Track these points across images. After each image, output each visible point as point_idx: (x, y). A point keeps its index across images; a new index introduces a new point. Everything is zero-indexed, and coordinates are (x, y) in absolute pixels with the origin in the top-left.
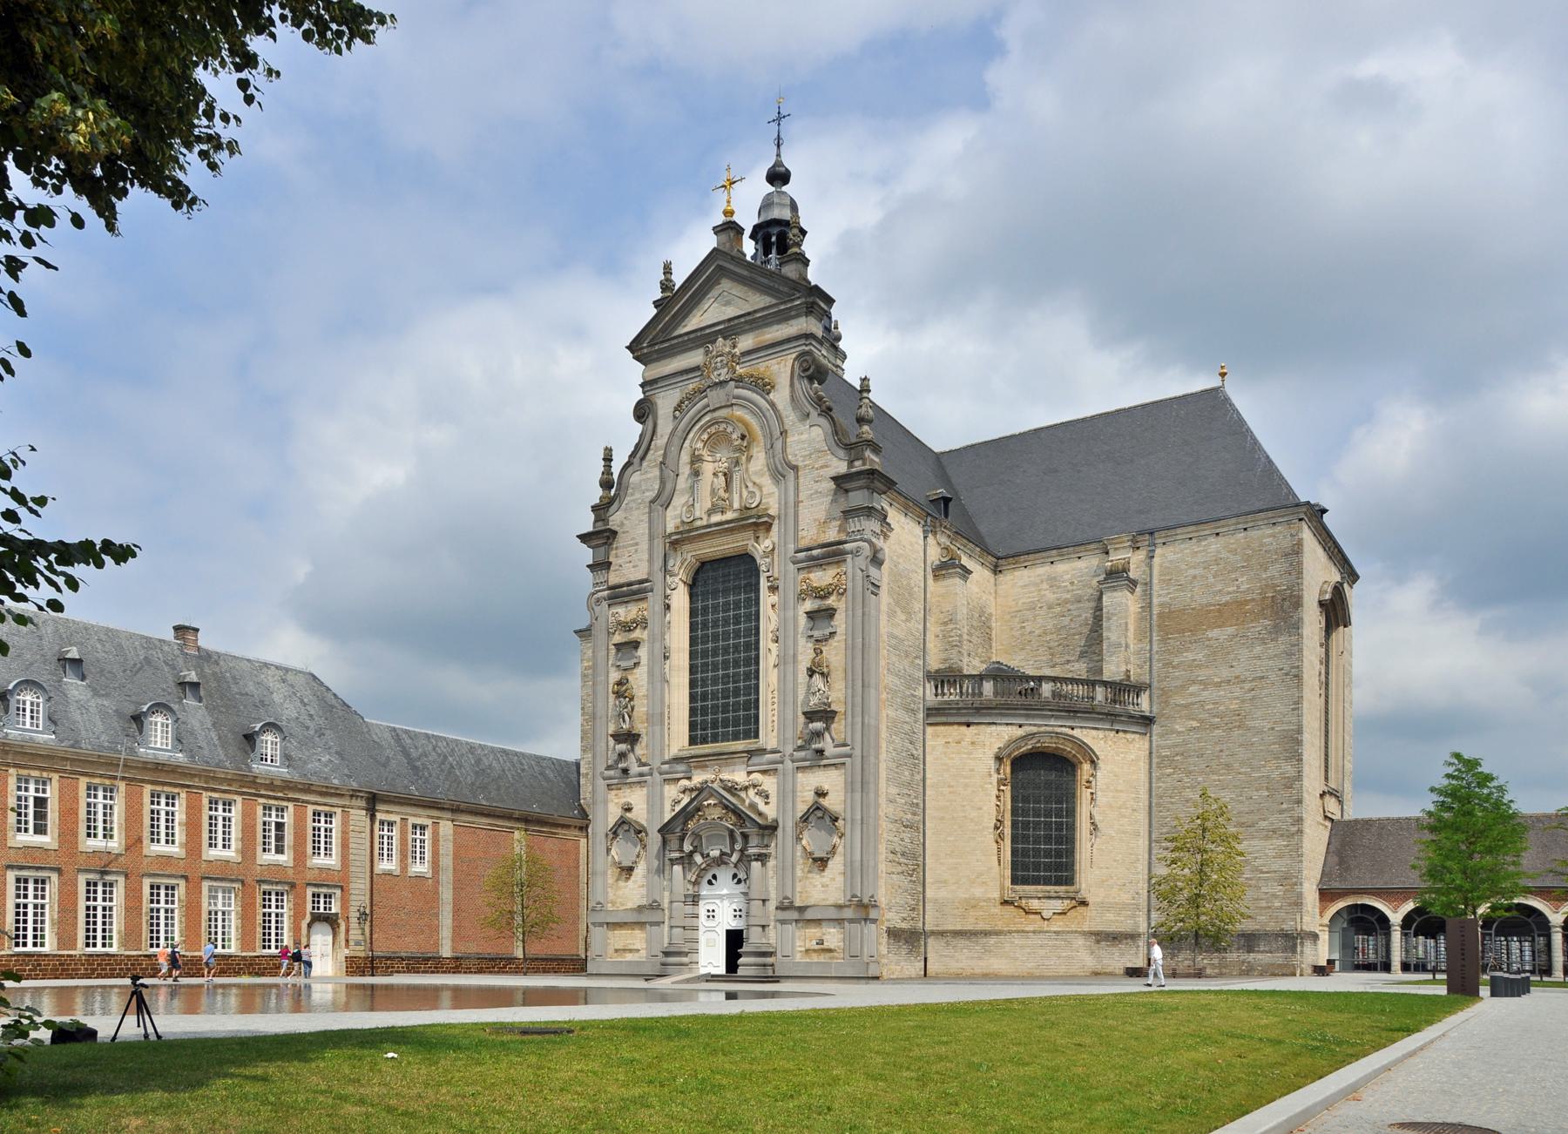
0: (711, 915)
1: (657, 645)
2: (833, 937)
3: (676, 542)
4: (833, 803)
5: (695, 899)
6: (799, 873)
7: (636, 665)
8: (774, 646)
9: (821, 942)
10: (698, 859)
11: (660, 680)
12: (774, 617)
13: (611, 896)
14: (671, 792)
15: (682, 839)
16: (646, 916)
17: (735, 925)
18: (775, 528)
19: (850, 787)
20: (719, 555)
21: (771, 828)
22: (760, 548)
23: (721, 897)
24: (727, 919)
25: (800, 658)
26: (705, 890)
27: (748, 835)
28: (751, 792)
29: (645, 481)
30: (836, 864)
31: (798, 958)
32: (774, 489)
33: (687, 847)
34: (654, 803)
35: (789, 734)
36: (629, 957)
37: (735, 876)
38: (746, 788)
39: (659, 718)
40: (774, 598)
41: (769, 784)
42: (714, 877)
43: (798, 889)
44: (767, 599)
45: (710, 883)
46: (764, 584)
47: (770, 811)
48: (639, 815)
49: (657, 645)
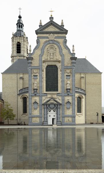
0: (50, 116)
1: (41, 77)
2: (70, 119)
3: (44, 62)
4: (70, 101)
5: (47, 114)
6: (65, 110)
7: (37, 79)
8: (61, 79)
9: (69, 120)
10: (49, 108)
11: (41, 81)
12: (61, 75)
13: (33, 113)
14: (44, 98)
15: (47, 105)
16: (40, 117)
17: (54, 117)
18: (61, 63)
19: (73, 99)
20: (51, 65)
21: (60, 104)
22: (59, 65)
23: (52, 113)
24: (52, 117)
25: (65, 81)
26: (49, 112)
27: (57, 106)
28: (57, 99)
29: (38, 52)
30: (71, 109)
31: (65, 122)
32: (60, 57)
33: (47, 106)
34: (41, 100)
35: (63, 91)
36: (36, 122)
37: (54, 111)
38: (57, 98)
39: (41, 87)
40: (61, 72)
41: (60, 98)
42: (50, 111)
43: (65, 113)
44: (59, 73)
45: (50, 111)
46: (59, 70)
47: (61, 102)
48: (38, 101)
49: (41, 77)
